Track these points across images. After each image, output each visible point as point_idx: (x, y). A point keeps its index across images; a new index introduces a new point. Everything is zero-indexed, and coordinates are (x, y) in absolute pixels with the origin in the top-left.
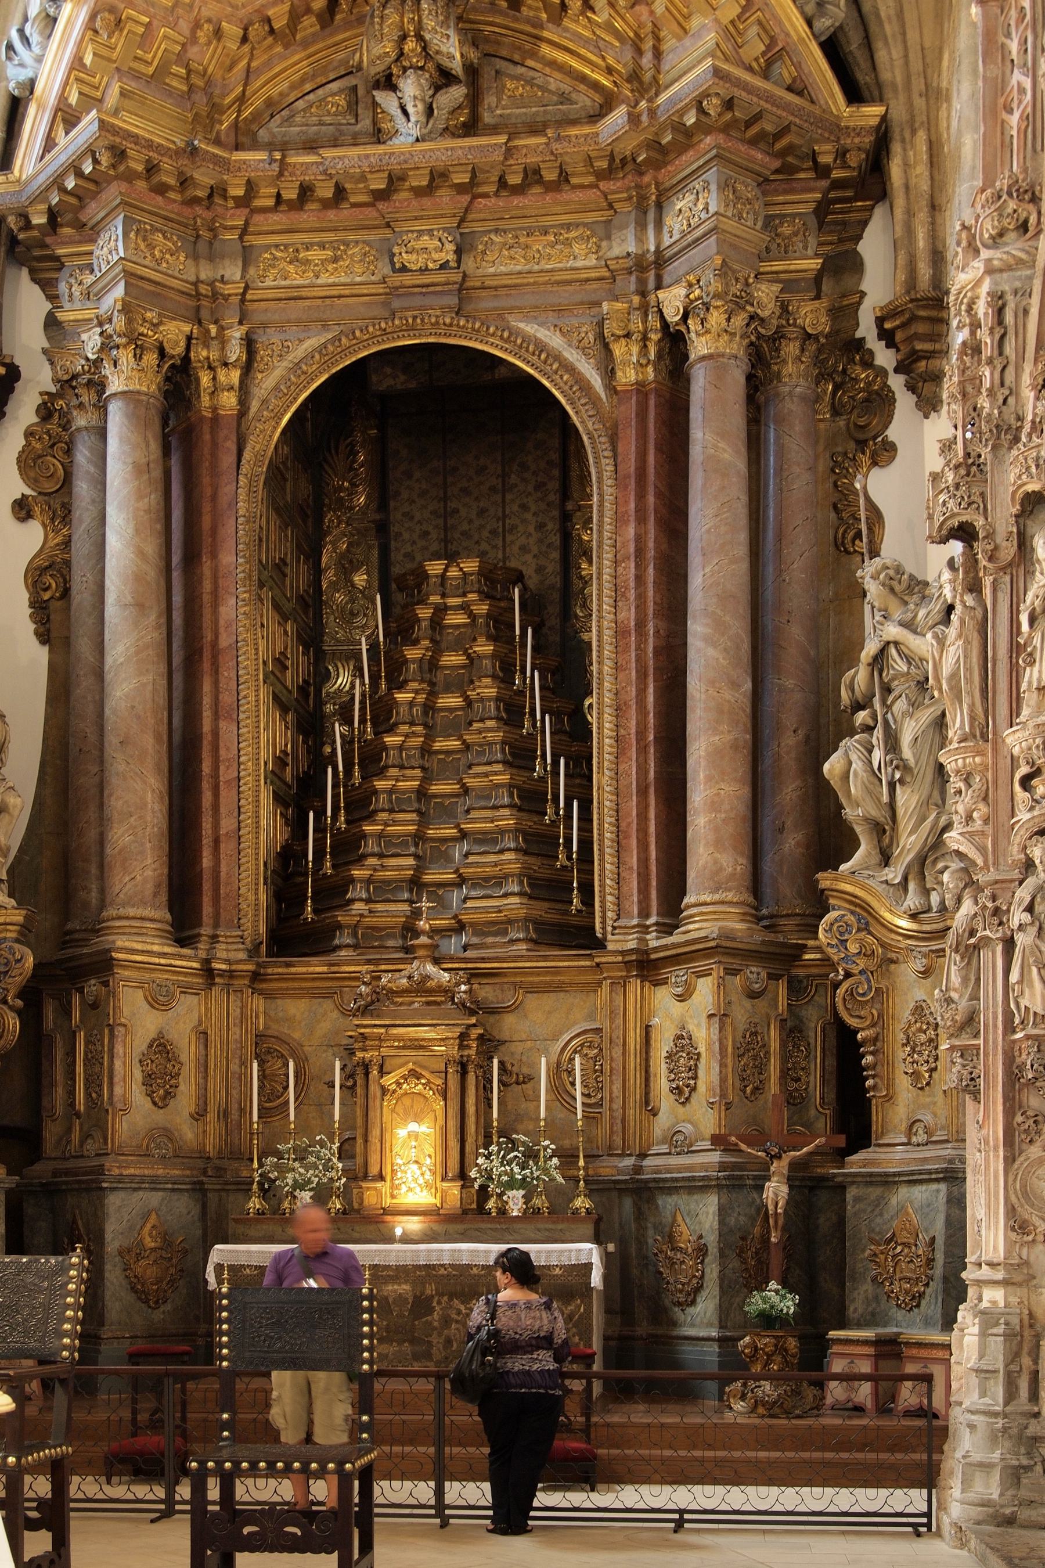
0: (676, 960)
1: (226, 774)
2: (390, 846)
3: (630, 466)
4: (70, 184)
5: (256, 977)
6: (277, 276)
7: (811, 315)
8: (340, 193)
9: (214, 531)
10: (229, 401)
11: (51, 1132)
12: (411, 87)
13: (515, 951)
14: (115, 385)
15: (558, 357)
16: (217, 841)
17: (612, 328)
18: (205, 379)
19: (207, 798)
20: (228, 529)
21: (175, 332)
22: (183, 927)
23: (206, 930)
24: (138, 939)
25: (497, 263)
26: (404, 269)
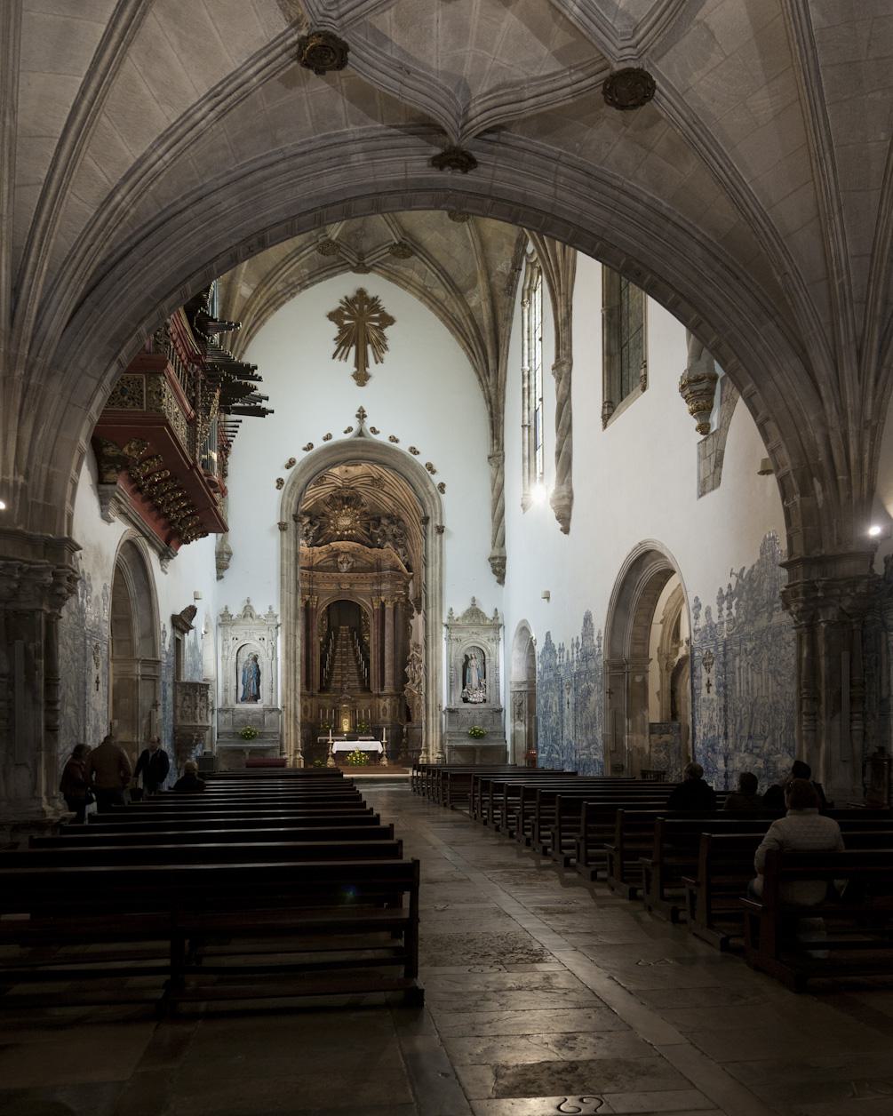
2: (337, 674)
7: (403, 600)
10: (315, 607)
13: (358, 693)
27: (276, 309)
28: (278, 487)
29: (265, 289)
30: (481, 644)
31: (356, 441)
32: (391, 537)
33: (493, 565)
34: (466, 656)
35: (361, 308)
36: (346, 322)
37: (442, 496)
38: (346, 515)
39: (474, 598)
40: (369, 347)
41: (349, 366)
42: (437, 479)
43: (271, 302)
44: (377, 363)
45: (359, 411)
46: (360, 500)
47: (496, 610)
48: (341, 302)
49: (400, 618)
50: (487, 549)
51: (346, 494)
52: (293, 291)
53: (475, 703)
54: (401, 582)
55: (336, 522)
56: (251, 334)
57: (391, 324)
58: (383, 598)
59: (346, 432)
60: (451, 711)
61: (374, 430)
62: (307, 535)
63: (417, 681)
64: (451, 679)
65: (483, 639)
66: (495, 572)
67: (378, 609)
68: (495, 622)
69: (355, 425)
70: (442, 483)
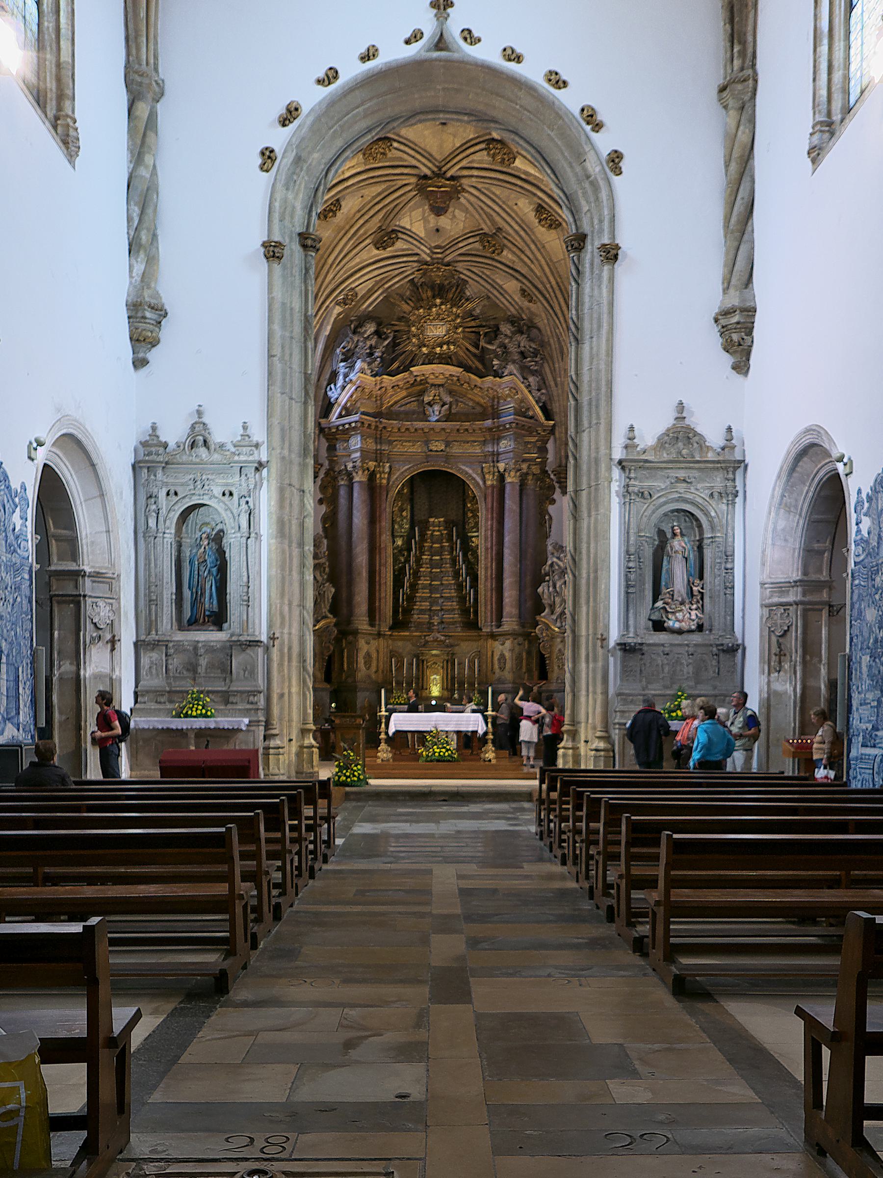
0: (500, 635)
1: (383, 581)
3: (490, 506)
4: (347, 426)
5: (391, 635)
6: (398, 448)
7: (536, 470)
8: (416, 430)
9: (380, 516)
11: (334, 675)
12: (436, 408)
14: (357, 479)
15: (470, 476)
16: (380, 599)
17: (485, 470)
18: (378, 476)
19: (377, 587)
20: (384, 516)
21: (372, 464)
22: (372, 622)
23: (377, 623)
25: (456, 450)
26: (431, 451)
30: (693, 503)
31: (431, 61)
32: (516, 357)
33: (724, 331)
34: (661, 533)
37: (616, 180)
38: (438, 317)
39: (681, 403)
42: (603, 143)
46: (462, 291)
47: (729, 429)
49: (530, 501)
50: (710, 296)
51: (438, 276)
53: (680, 632)
54: (533, 439)
55: (422, 329)
58: (501, 466)
59: (408, 42)
60: (626, 649)
61: (469, 36)
62: (371, 354)
63: (558, 610)
64: (627, 579)
65: (699, 492)
66: (728, 347)
67: (492, 486)
68: (727, 456)
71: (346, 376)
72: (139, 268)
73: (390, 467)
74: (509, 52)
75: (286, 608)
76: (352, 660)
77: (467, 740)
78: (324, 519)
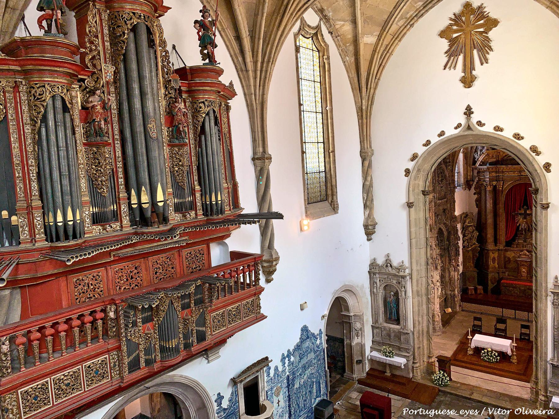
24: (490, 246)
27: (400, 41)
28: (406, 176)
29: (385, 33)
35: (468, 19)
36: (455, 35)
40: (475, 52)
41: (458, 72)
43: (396, 37)
44: (482, 64)
45: (466, 109)
48: (451, 19)
52: (411, 23)
56: (383, 64)
57: (496, 26)
59: (456, 128)
61: (480, 123)
64: (554, 339)
69: (462, 120)
70: (548, 163)
71: (481, 151)
72: (367, 213)
73: (503, 183)
74: (497, 129)
75: (420, 319)
76: (487, 261)
77: (503, 355)
78: (477, 200)
